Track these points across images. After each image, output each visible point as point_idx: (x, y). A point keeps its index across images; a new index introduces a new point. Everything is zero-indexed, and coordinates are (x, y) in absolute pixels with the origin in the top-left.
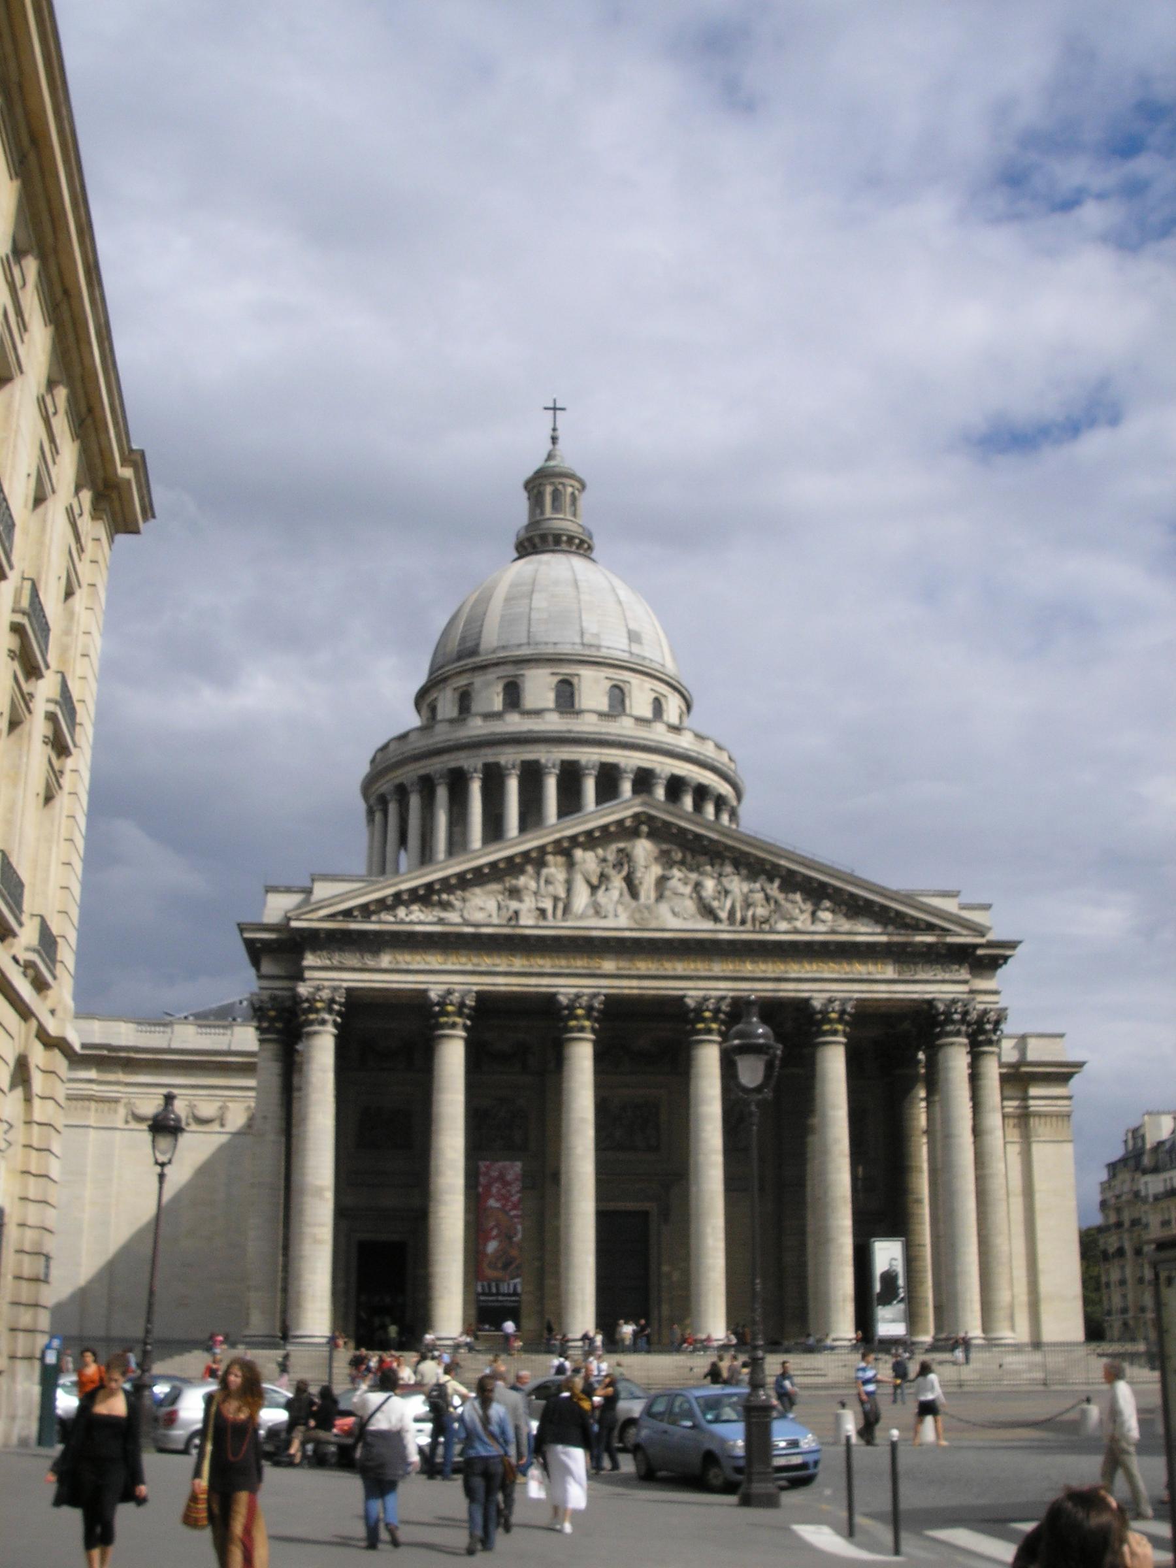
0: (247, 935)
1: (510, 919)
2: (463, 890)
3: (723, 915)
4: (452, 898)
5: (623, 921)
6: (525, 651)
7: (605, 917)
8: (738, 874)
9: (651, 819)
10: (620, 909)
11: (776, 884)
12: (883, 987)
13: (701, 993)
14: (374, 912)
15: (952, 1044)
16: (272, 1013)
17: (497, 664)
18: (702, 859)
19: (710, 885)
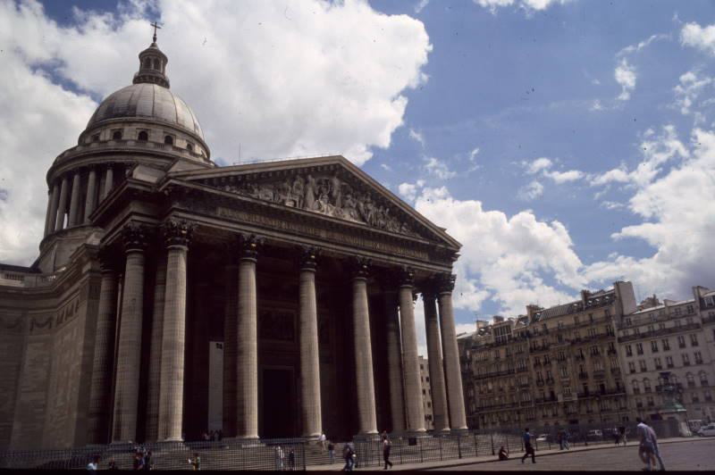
5: (330, 214)
9: (341, 167)
11: (388, 210)
12: (425, 265)
14: (213, 185)
16: (142, 236)
18: (359, 193)
19: (362, 205)
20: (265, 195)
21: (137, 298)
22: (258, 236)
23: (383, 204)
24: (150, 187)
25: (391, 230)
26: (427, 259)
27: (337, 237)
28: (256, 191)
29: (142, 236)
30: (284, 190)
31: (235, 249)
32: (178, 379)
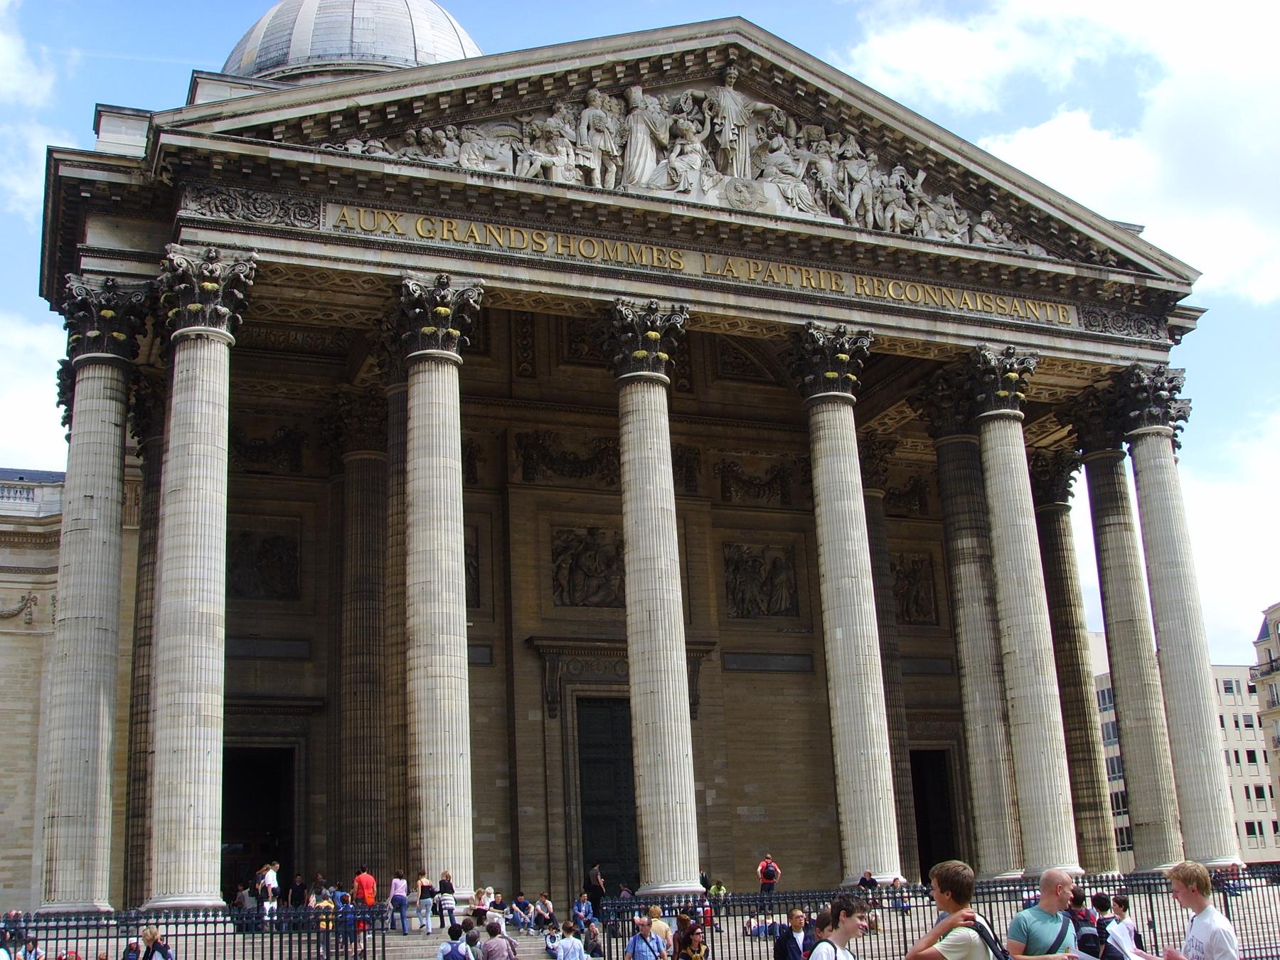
0: (64, 171)
1: (536, 176)
2: (459, 126)
3: (851, 213)
4: (440, 133)
6: (348, 62)
7: (686, 192)
8: (866, 158)
9: (747, 56)
10: (708, 183)
12: (1068, 344)
13: (833, 326)
14: (305, 139)
15: (1158, 434)
16: (108, 313)
17: (311, 75)
18: (816, 131)
19: (826, 166)
20: (479, 157)
21: (99, 493)
22: (457, 284)
23: (904, 159)
24: (126, 171)
25: (936, 236)
26: (1074, 325)
27: (743, 271)
28: (451, 146)
29: (108, 313)
30: (548, 136)
31: (389, 330)
32: (201, 720)
